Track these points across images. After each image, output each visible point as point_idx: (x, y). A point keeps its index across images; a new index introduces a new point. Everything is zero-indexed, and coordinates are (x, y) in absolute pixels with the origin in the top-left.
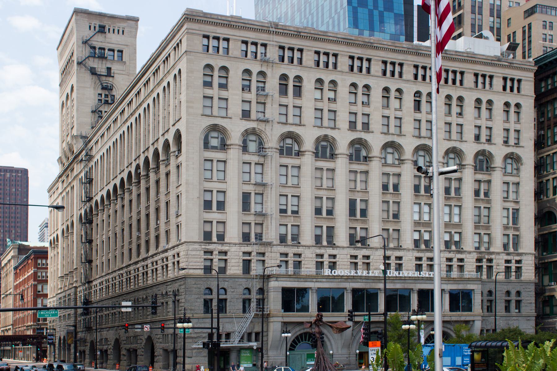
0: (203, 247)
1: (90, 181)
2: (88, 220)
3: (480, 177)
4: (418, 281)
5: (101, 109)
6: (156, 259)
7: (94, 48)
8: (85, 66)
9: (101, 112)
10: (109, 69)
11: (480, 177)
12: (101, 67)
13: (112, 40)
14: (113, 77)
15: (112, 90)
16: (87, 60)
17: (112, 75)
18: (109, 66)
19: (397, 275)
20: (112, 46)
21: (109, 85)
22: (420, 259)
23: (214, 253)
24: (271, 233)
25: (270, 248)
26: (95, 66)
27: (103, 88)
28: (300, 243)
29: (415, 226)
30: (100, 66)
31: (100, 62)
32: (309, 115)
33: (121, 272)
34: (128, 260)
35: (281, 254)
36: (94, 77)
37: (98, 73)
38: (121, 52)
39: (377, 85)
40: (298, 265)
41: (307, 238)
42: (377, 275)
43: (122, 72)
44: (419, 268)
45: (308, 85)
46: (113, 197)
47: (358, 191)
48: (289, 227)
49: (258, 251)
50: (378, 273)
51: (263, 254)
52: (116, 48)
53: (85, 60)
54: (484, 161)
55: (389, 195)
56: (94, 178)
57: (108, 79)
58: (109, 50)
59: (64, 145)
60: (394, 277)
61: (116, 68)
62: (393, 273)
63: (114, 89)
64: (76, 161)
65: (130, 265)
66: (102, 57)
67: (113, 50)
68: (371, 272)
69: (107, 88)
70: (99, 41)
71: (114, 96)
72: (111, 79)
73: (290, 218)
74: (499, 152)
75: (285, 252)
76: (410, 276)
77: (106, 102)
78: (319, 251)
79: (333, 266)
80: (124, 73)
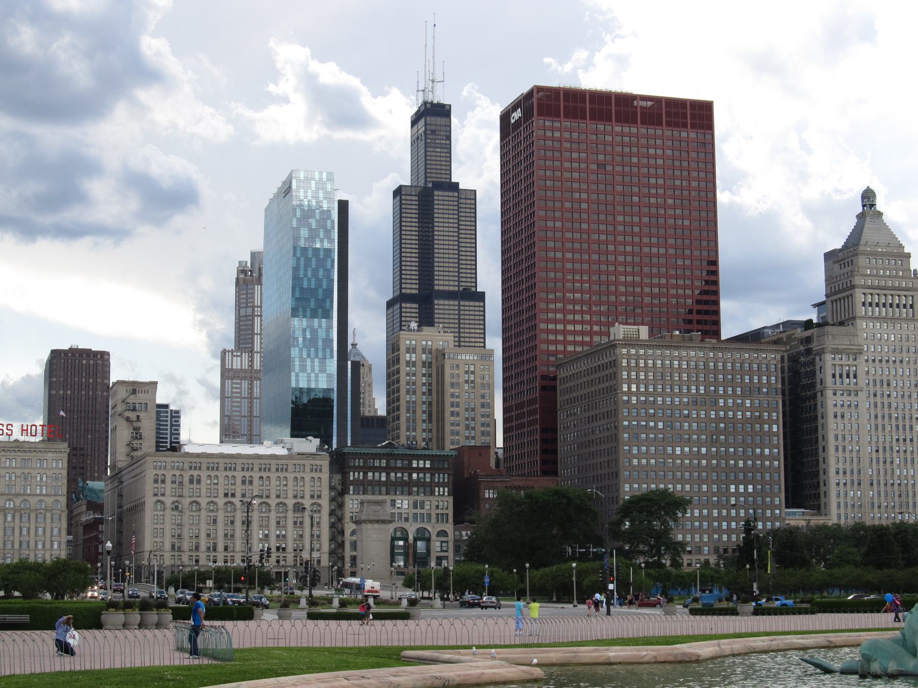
3: (297, 515)
10: (138, 416)
11: (297, 515)
12: (132, 415)
13: (141, 397)
24: (186, 546)
32: (204, 491)
39: (239, 475)
40: (197, 561)
41: (203, 547)
45: (203, 479)
52: (143, 402)
54: (299, 508)
61: (142, 415)
66: (134, 410)
69: (137, 429)
70: (132, 399)
74: (307, 503)
77: (136, 438)
79: (215, 562)
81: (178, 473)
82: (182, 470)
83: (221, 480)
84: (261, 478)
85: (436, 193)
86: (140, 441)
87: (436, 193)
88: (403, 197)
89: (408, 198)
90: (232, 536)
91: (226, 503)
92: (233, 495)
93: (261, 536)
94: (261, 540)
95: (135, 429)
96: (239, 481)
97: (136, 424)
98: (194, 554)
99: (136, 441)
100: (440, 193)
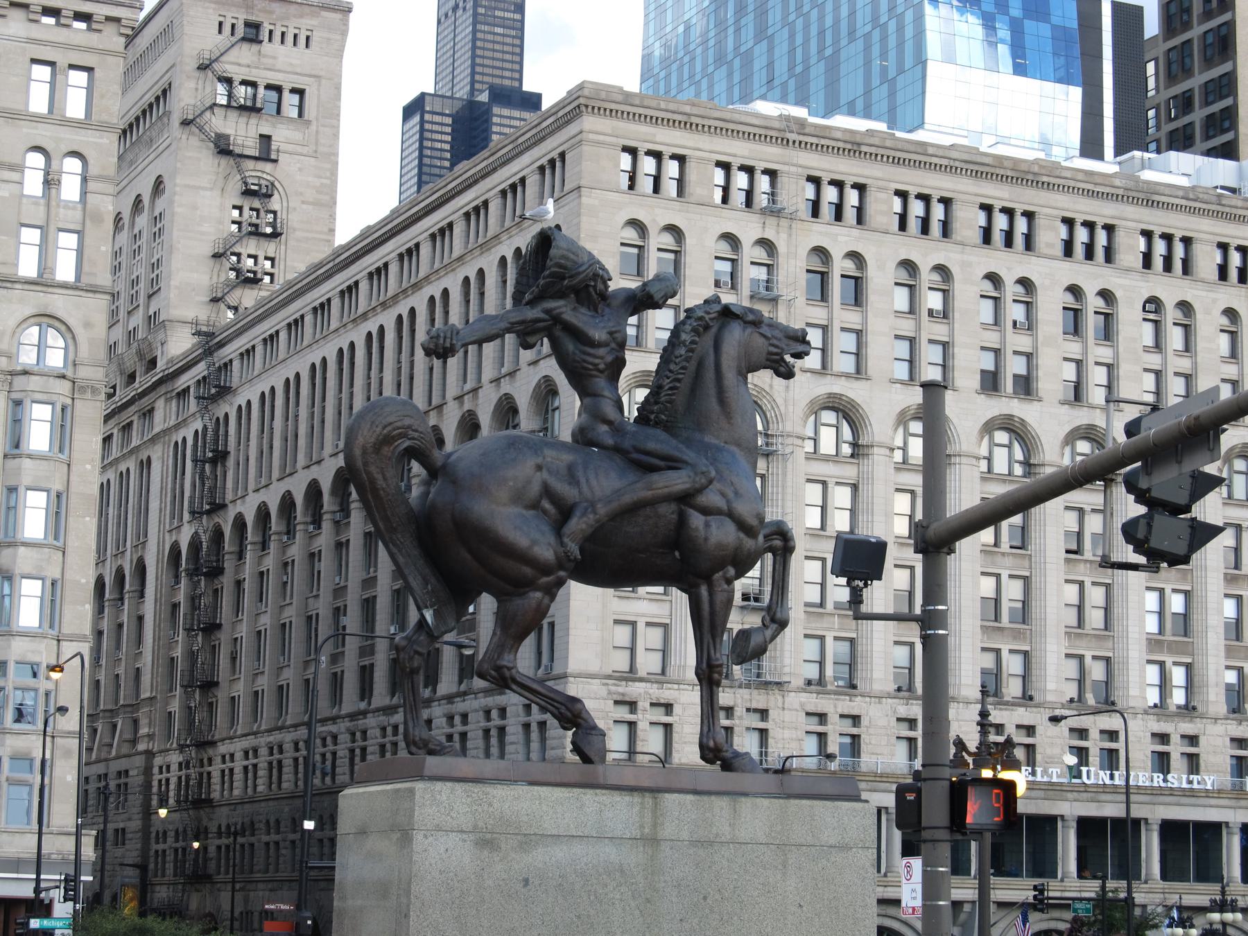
0: (613, 688)
1: (220, 457)
2: (203, 564)
4: (1162, 799)
5: (237, 249)
6: (460, 706)
7: (228, 81)
8: (201, 129)
9: (238, 255)
10: (266, 139)
14: (276, 161)
15: (270, 196)
16: (208, 114)
17: (273, 157)
18: (265, 131)
19: (1108, 781)
20: (275, 78)
21: (263, 183)
22: (1163, 738)
23: (640, 705)
25: (780, 698)
26: (229, 130)
27: (248, 193)
28: (854, 687)
29: (1150, 651)
30: (241, 132)
31: (243, 120)
33: (333, 728)
34: (356, 698)
35: (808, 714)
36: (225, 161)
37: (237, 150)
38: (300, 92)
42: (1055, 780)
43: (299, 149)
44: (1162, 762)
46: (305, 515)
47: (1003, 554)
48: (829, 642)
49: (748, 706)
50: (1056, 775)
51: (764, 714)
52: (287, 82)
53: (203, 112)
55: (1082, 565)
56: (232, 446)
57: (261, 165)
58: (269, 87)
59: (118, 333)
60: (1097, 785)
61: (282, 135)
62: (1097, 775)
63: (276, 196)
64: (162, 389)
65: (364, 713)
66: (251, 109)
67: (278, 89)
68: (1039, 770)
69: (257, 193)
71: (275, 213)
72: (268, 167)
73: (831, 619)
75: (819, 710)
76: (1140, 784)
77: (256, 232)
78: (903, 711)
80: (305, 150)
81: (749, 229)
82: (774, 211)
83: (968, 290)
84: (1153, 304)
85: (496, 110)
86: (271, 248)
87: (496, 110)
88: (427, 117)
89: (437, 119)
90: (1024, 613)
91: (989, 428)
92: (1026, 386)
93: (1152, 625)
94: (1154, 643)
95: (257, 193)
96: (1051, 304)
97: (258, 172)
98: (835, 706)
99: (251, 246)
100: (506, 112)
